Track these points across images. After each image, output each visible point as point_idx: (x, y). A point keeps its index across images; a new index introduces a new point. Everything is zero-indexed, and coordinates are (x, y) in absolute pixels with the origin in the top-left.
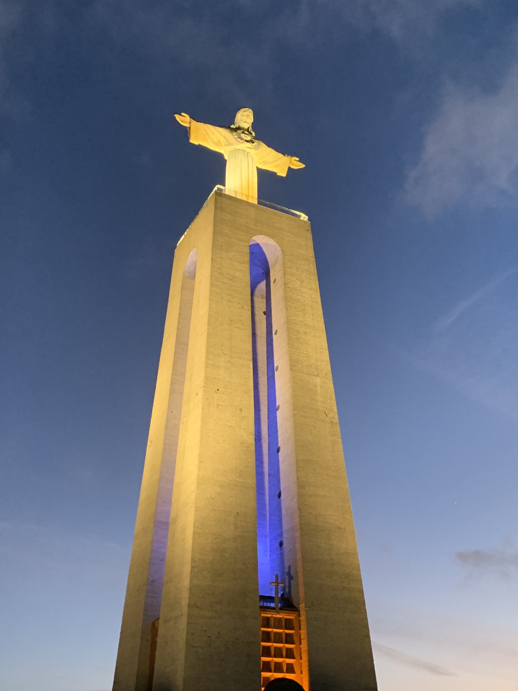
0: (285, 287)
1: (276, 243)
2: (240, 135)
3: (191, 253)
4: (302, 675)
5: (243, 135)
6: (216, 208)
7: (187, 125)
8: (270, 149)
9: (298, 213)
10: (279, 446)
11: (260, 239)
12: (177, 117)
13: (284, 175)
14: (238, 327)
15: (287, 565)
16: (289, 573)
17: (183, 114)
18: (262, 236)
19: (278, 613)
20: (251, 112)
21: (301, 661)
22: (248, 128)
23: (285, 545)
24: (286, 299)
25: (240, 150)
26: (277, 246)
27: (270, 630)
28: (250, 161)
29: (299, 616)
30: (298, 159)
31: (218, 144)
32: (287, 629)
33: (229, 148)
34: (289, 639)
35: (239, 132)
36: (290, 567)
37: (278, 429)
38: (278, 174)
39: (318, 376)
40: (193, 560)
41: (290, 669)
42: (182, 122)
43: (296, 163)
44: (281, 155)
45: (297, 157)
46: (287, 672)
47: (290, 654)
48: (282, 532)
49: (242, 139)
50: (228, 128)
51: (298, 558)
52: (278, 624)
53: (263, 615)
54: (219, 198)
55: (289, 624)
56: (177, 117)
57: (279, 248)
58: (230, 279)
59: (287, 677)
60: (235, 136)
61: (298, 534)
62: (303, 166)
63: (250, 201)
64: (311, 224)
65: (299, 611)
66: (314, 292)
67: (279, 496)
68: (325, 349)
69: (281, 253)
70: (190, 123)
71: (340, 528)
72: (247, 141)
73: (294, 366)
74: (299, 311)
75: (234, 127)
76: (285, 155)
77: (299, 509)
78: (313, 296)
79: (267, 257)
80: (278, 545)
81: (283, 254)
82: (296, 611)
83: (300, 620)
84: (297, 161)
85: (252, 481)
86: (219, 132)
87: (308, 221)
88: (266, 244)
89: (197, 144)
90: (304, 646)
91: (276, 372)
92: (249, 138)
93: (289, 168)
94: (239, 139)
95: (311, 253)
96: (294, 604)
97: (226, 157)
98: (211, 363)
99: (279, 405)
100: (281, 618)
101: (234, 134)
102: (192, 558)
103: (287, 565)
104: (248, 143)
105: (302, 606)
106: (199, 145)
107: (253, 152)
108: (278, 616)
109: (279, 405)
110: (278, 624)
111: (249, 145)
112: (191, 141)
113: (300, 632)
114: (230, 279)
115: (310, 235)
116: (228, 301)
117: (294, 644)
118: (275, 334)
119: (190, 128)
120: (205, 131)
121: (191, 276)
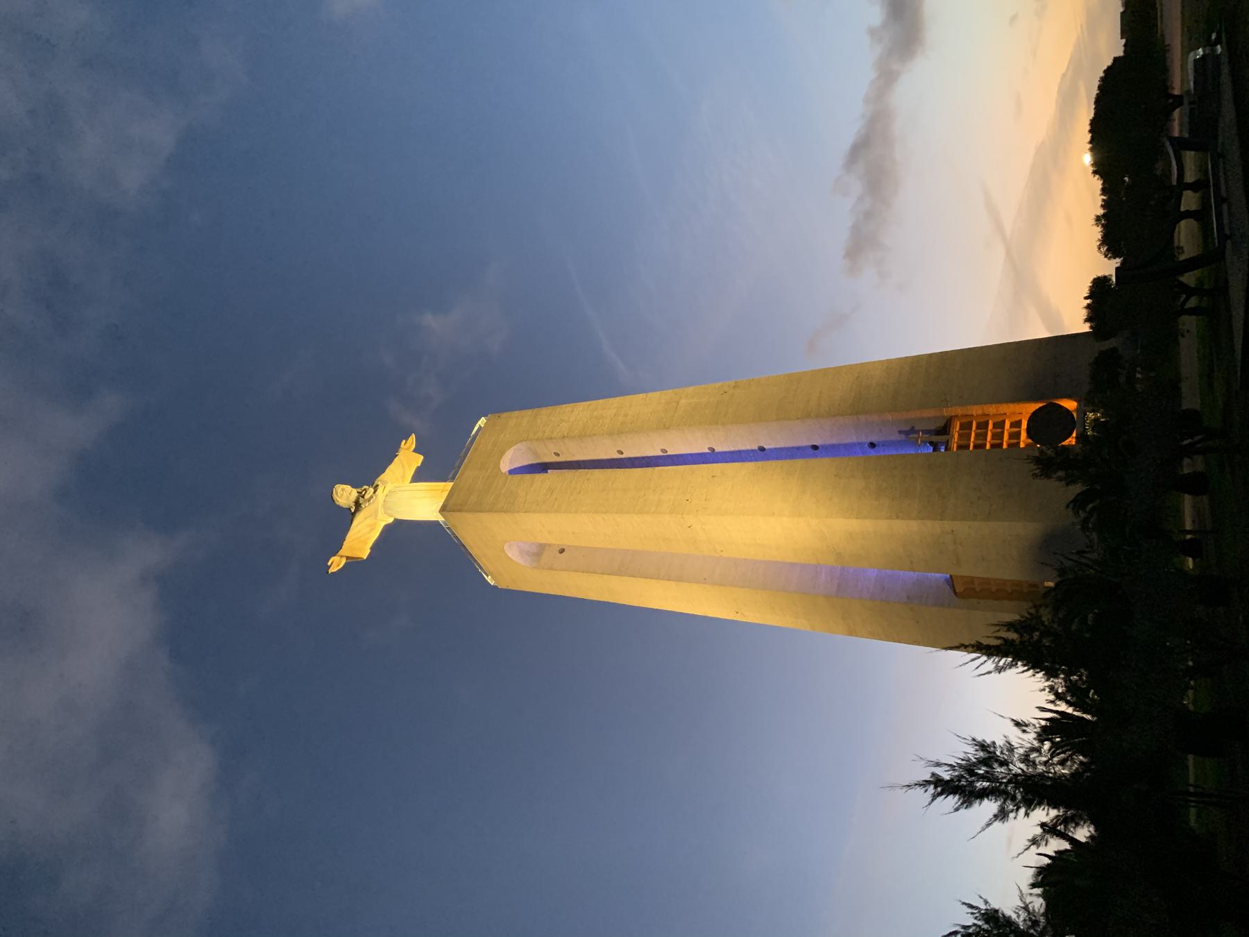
0: (568, 437)
1: (513, 448)
2: (366, 500)
3: (509, 555)
4: (1024, 413)
5: (367, 496)
6: (460, 511)
7: (344, 561)
8: (387, 470)
9: (476, 428)
10: (756, 448)
11: (505, 466)
12: (333, 569)
13: (421, 458)
14: (613, 483)
15: (897, 437)
16: (907, 433)
17: (329, 564)
18: (501, 462)
19: (953, 436)
20: (339, 487)
21: (1008, 414)
22: (358, 492)
23: (874, 439)
24: (583, 436)
25: (384, 501)
26: (515, 447)
27: (972, 444)
28: (399, 489)
29: (957, 416)
30: (404, 441)
31: (372, 528)
32: (971, 429)
33: (380, 515)
34: (983, 426)
35: (361, 500)
36: (900, 432)
37: (737, 449)
38: (419, 465)
39: (678, 403)
40: (890, 518)
41: (1017, 424)
42: (338, 566)
43: (408, 444)
44: (396, 459)
45: (402, 441)
46: (1020, 427)
47: (1000, 425)
48: (859, 443)
49: (372, 497)
50: (354, 514)
51: (890, 418)
52: (965, 436)
53: (955, 450)
54: (448, 508)
55: (966, 427)
56: (333, 569)
57: (519, 444)
58: (551, 494)
59: (1026, 427)
60: (367, 504)
61: (862, 418)
62: (413, 436)
63: (449, 488)
64: (492, 413)
65: (951, 417)
66: (575, 409)
67: (815, 447)
68: (647, 396)
69: (524, 443)
70: (342, 556)
71: (858, 377)
72: (374, 492)
73: (664, 425)
74: (599, 423)
75: (354, 508)
76: (397, 455)
77: (834, 416)
78: (581, 409)
79: (526, 463)
80: (872, 450)
81: (526, 441)
82: (950, 422)
83: (962, 416)
84: (406, 442)
85: (799, 463)
86: (357, 526)
87: (487, 416)
88: (511, 461)
89: (369, 551)
90: (991, 409)
91: (668, 453)
92: (372, 490)
93: (415, 451)
94: (371, 501)
95: (528, 414)
96: (942, 425)
97: (391, 520)
98: (653, 509)
99: (709, 448)
100: (959, 435)
101: (363, 506)
102: (887, 519)
103: (897, 437)
104: (378, 490)
105: (947, 412)
106: (372, 548)
107: (389, 487)
108: (956, 436)
109: (709, 448)
110: (965, 436)
111: (380, 490)
112: (365, 558)
113: (975, 415)
114: (551, 494)
115: (505, 415)
116: (579, 494)
117: (988, 421)
118: (622, 453)
119: (348, 558)
120: (354, 540)
121: (538, 552)
